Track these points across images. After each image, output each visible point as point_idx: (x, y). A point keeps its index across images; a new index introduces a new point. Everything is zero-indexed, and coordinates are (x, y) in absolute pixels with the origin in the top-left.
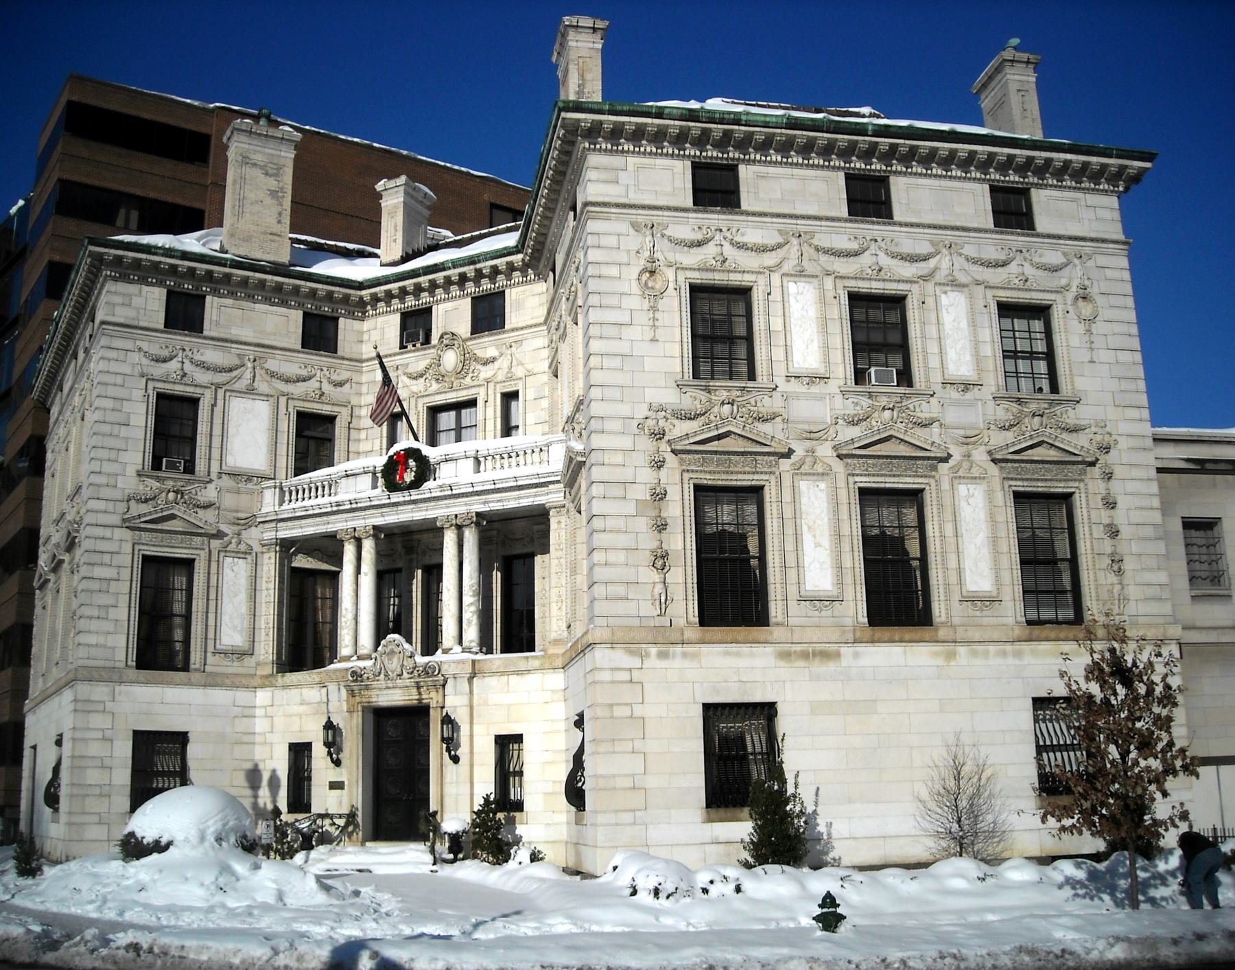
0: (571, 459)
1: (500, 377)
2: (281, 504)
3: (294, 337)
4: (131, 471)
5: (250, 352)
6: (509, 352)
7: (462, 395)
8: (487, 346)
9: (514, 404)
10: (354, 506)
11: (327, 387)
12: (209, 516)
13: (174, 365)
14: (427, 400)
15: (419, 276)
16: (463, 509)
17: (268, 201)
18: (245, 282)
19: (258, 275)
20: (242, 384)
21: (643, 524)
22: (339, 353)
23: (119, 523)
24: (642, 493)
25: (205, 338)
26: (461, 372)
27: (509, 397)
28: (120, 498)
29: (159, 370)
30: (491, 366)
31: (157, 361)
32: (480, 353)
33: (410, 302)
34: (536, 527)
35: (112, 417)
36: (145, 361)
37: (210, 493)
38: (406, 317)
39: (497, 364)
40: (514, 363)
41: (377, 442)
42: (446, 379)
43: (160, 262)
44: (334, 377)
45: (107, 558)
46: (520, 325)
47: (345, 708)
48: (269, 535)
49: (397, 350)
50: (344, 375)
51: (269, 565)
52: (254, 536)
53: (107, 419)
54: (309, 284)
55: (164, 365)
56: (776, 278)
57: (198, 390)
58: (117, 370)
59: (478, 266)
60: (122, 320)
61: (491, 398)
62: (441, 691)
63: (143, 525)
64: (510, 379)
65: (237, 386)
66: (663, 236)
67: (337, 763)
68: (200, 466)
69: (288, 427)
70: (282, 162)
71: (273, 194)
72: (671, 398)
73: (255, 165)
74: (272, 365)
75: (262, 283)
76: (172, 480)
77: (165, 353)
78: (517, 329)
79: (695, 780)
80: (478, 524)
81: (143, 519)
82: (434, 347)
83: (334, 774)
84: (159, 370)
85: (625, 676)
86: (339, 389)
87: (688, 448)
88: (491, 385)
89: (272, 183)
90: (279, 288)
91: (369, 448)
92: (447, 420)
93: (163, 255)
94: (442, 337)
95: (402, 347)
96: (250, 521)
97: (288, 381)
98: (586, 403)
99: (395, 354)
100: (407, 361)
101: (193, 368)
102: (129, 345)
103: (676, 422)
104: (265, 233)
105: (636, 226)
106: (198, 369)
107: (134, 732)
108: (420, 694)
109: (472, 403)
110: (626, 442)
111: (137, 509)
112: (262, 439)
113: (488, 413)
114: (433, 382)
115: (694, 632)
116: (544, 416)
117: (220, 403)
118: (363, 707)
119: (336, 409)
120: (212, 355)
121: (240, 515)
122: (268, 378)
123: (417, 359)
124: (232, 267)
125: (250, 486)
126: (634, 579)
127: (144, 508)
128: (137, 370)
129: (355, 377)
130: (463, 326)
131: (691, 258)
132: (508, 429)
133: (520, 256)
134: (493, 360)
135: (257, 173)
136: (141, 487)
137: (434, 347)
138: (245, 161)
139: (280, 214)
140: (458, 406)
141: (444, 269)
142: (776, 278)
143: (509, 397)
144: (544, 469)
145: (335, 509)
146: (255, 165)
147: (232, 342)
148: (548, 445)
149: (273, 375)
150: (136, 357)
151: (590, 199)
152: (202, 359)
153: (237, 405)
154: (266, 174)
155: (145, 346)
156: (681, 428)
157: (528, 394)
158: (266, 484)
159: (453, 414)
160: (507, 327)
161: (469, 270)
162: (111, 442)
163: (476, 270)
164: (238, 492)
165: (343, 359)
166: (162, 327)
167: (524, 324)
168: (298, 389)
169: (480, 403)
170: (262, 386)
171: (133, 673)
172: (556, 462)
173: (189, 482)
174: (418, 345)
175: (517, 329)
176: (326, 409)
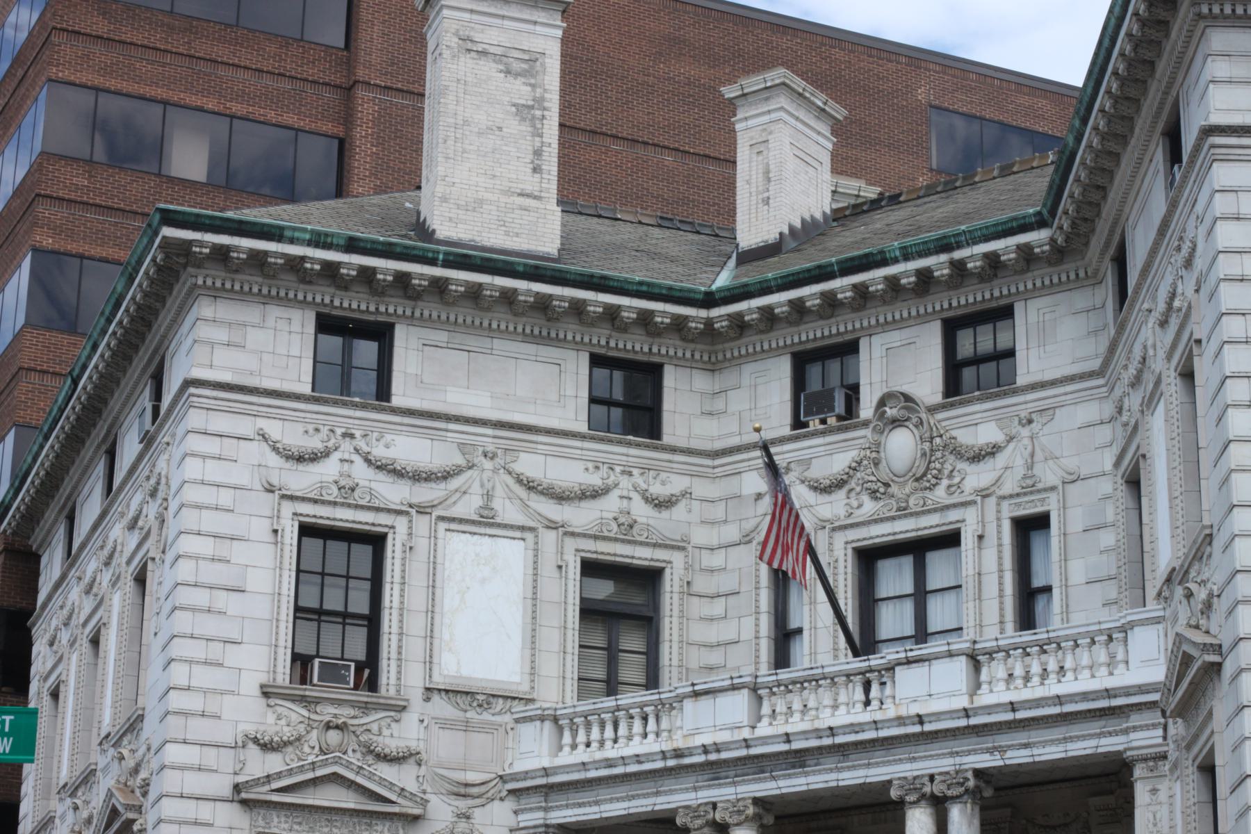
0: (1187, 660)
1: (1009, 487)
3: (571, 410)
4: (250, 685)
5: (486, 438)
6: (1025, 432)
7: (930, 524)
8: (978, 424)
9: (1036, 540)
10: (713, 757)
11: (641, 511)
12: (405, 777)
13: (329, 469)
14: (853, 535)
15: (830, 276)
16: (944, 764)
17: (514, 126)
20: (468, 507)
22: (667, 439)
23: (227, 792)
26: (924, 477)
27: (1030, 528)
28: (229, 740)
29: (302, 479)
30: (988, 464)
31: (300, 459)
32: (966, 437)
33: (813, 333)
34: (1095, 801)
35: (211, 573)
36: (274, 460)
38: (802, 361)
39: (1001, 459)
40: (1039, 456)
41: (749, 622)
42: (894, 489)
43: (303, 259)
44: (657, 489)
46: (1049, 376)
49: (787, 431)
50: (676, 484)
53: (202, 579)
57: (384, 519)
58: (219, 479)
59: (958, 255)
60: (226, 377)
61: (991, 531)
63: (276, 798)
65: (459, 511)
69: (566, 592)
70: (536, 44)
71: (524, 111)
73: (484, 53)
74: (530, 464)
75: (508, 297)
76: (337, 705)
77: (315, 443)
78: (1042, 385)
80: (974, 794)
81: (275, 785)
82: (866, 424)
84: (302, 479)
86: (665, 514)
89: (520, 90)
90: (543, 305)
91: (732, 636)
92: (895, 578)
93: (309, 243)
94: (882, 403)
95: (798, 424)
97: (561, 497)
98: (1218, 543)
100: (805, 454)
101: (370, 473)
102: (245, 426)
104: (508, 192)
106: (381, 476)
109: (950, 540)
111: (259, 764)
112: (514, 618)
113: (985, 563)
114: (865, 498)
116: (1108, 565)
117: (422, 544)
119: (661, 554)
120: (409, 448)
121: (472, 777)
122: (522, 492)
123: (829, 454)
124: (447, 264)
125: (486, 716)
127: (275, 763)
132: (1029, 600)
134: (993, 451)
135: (488, 68)
136: (271, 718)
137: (866, 424)
138: (468, 46)
139: (538, 153)
140: (918, 549)
143: (1030, 528)
144: (1123, 678)
146: (484, 53)
148: (1125, 629)
149: (530, 486)
151: (1217, 119)
153: (461, 550)
154: (508, 72)
155: (274, 429)
157: (1070, 518)
159: (907, 562)
160: (1021, 381)
161: (937, 263)
162: (209, 626)
163: (953, 263)
164: (467, 727)
165: (673, 450)
166: (306, 389)
168: (581, 516)
169: (968, 540)
170: (508, 511)
172: (1145, 663)
173: (366, 708)
174: (832, 421)
175: (1042, 385)
176: (641, 556)
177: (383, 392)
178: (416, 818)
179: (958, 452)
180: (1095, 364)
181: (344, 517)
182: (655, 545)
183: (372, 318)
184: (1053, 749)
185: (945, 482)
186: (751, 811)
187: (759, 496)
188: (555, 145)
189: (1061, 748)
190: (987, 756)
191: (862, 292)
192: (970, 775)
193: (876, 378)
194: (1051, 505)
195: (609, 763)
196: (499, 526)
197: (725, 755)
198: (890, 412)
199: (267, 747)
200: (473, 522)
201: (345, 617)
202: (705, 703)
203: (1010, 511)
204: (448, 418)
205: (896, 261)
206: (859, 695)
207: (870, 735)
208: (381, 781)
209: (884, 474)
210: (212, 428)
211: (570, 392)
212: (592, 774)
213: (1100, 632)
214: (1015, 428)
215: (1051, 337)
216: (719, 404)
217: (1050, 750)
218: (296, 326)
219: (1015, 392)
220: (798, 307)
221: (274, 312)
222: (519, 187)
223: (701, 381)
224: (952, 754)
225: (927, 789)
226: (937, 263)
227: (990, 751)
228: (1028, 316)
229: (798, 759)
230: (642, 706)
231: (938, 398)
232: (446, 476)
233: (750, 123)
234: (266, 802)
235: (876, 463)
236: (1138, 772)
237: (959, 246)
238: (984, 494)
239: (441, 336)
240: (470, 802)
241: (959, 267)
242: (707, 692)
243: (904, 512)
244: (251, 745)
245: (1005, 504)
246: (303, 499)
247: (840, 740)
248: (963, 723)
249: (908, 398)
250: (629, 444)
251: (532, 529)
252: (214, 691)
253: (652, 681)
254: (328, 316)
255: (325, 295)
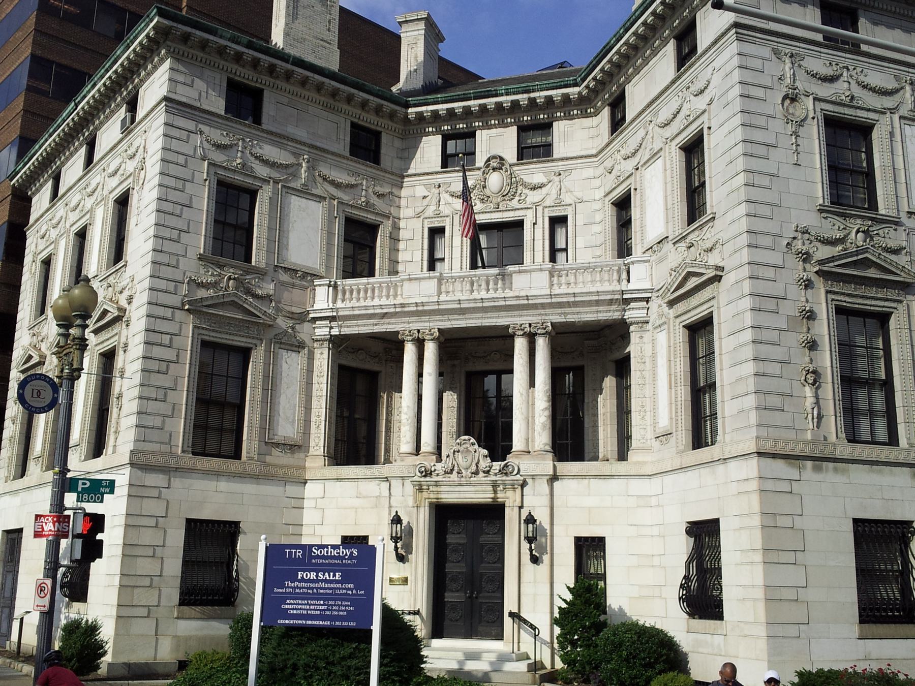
1: (547, 203)
2: (335, 301)
4: (192, 254)
6: (557, 179)
8: (534, 172)
10: (420, 308)
16: (533, 319)
18: (304, 82)
19: (317, 76)
20: (297, 184)
21: (794, 340)
24: (790, 309)
25: (263, 131)
27: (558, 222)
29: (219, 157)
32: (527, 179)
37: (268, 288)
39: (544, 190)
44: (378, 189)
45: (166, 339)
47: (410, 501)
48: (322, 331)
49: (439, 169)
51: (322, 359)
52: (304, 331)
54: (361, 94)
55: (227, 152)
56: (896, 117)
59: (532, 95)
60: (184, 100)
62: (519, 491)
63: (204, 310)
64: (559, 204)
66: (800, 66)
67: (401, 558)
68: (258, 257)
72: (812, 220)
78: (567, 159)
79: (846, 593)
81: (204, 304)
83: (396, 570)
85: (785, 487)
87: (834, 270)
88: (540, 209)
91: (409, 259)
94: (489, 160)
95: (444, 165)
96: (302, 317)
97: (337, 185)
99: (436, 173)
101: (253, 159)
103: (819, 245)
104: (317, 38)
105: (776, 52)
106: (257, 162)
107: (189, 521)
108: (495, 492)
110: (775, 258)
115: (845, 450)
118: (431, 504)
120: (270, 151)
126: (788, 391)
128: (199, 151)
129: (395, 191)
130: (511, 155)
131: (825, 90)
133: (576, 90)
136: (202, 271)
137: (479, 169)
141: (496, 95)
142: (896, 117)
143: (558, 222)
145: (398, 310)
147: (289, 139)
150: (198, 140)
152: (261, 151)
156: (824, 252)
158: (317, 282)
160: (555, 156)
161: (523, 98)
163: (529, 99)
167: (575, 155)
171: (189, 460)
173: (247, 272)
175: (567, 159)
176: (371, 218)
177: (257, 121)
178: (270, 326)
179: (525, 185)
180: (594, 152)
181: (239, 178)
182: (377, 214)
183: (254, 84)
184: (591, 315)
185: (517, 198)
186: (437, 334)
187: (424, 197)
188: (337, 20)
189: (595, 315)
190: (558, 317)
191: (483, 107)
192: (549, 324)
193: (484, 149)
194: (569, 212)
195: (366, 308)
196: (310, 194)
197: (426, 308)
198: (494, 163)
199: (201, 285)
200: (298, 190)
201: (236, 227)
202: (415, 284)
203: (549, 213)
204: (289, 139)
205: (502, 95)
206: (468, 287)
207: (502, 303)
208: (256, 307)
209: (487, 192)
210: (175, 124)
211: (342, 137)
212: (357, 312)
213: (607, 266)
214: (553, 177)
215: (574, 136)
216: (406, 155)
217: (589, 315)
218: (217, 82)
219: (553, 160)
220: (451, 112)
221: (207, 73)
222: (321, 36)
223: (398, 143)
224: (539, 315)
225: (527, 330)
226: (523, 98)
227: (560, 314)
228: (560, 128)
229: (462, 311)
230: (380, 283)
231: (515, 161)
232: (287, 166)
233: (409, 34)
234: (200, 311)
235: (484, 187)
236: (632, 328)
237: (534, 91)
238: (537, 205)
239: (285, 100)
240: (293, 322)
241: (532, 101)
242: (416, 279)
243: (497, 209)
244: (192, 283)
245: (546, 210)
246: (220, 166)
247: (485, 304)
248: (549, 301)
249: (501, 159)
250: (367, 166)
251: (325, 198)
252: (174, 254)
253: (394, 272)
254: (233, 79)
255: (234, 67)
